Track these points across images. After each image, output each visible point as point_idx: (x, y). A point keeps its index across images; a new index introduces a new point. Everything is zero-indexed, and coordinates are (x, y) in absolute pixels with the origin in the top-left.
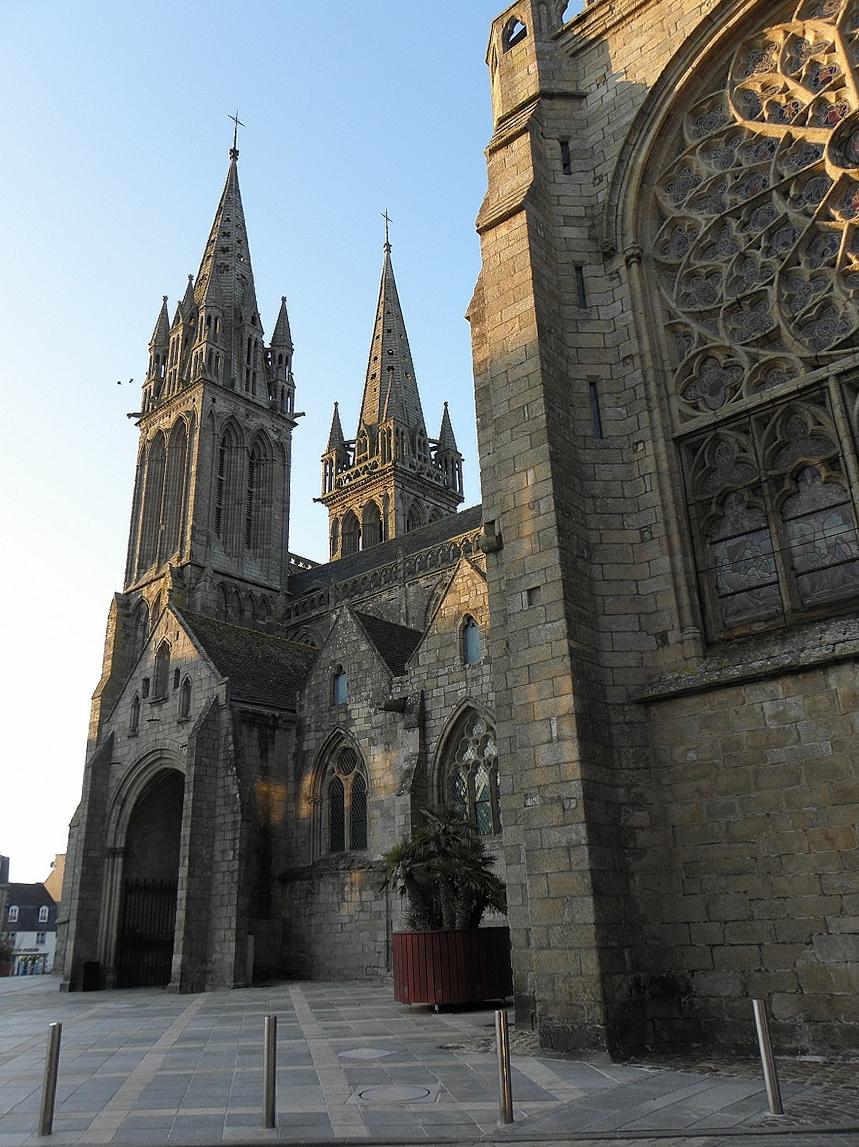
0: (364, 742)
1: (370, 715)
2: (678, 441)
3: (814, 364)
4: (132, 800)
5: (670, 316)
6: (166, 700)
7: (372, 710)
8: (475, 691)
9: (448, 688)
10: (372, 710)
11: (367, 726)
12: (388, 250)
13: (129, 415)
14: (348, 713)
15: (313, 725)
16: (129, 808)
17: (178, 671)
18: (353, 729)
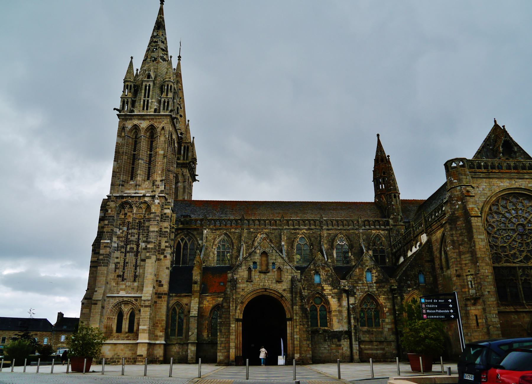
0: (330, 297)
1: (332, 289)
2: (493, 267)
3: (514, 263)
4: (247, 303)
5: (489, 242)
6: (268, 272)
7: (333, 288)
8: (371, 290)
9: (362, 287)
10: (333, 288)
11: (331, 292)
12: (179, 60)
13: (115, 109)
14: (323, 287)
15: (306, 288)
16: (245, 306)
17: (273, 264)
18: (325, 292)
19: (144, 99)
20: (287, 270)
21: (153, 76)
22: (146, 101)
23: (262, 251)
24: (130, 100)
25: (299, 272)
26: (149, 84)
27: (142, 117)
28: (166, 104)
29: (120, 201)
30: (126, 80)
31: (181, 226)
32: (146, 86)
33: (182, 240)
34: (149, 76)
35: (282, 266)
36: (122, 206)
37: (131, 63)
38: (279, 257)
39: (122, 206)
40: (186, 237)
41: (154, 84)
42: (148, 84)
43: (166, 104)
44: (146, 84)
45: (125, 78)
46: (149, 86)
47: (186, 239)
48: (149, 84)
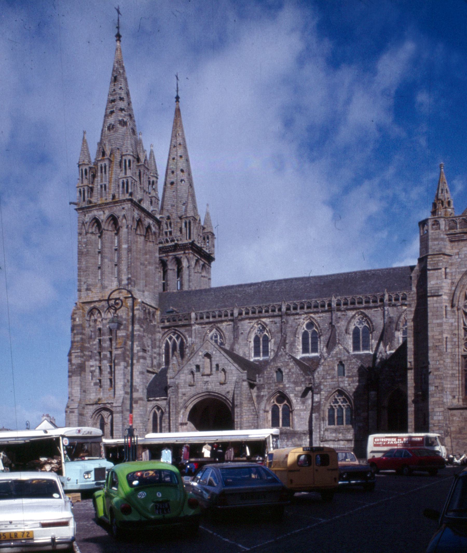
19: (101, 184)
20: (231, 371)
21: (108, 152)
22: (103, 186)
23: (204, 353)
24: (86, 188)
25: (246, 371)
26: (105, 164)
27: (101, 207)
28: (125, 186)
29: (87, 308)
30: (80, 163)
31: (167, 324)
32: (101, 168)
33: (170, 338)
34: (104, 154)
35: (226, 367)
36: (91, 312)
37: (84, 141)
38: (223, 357)
39: (91, 312)
40: (174, 335)
41: (111, 161)
42: (103, 166)
43: (125, 186)
44: (101, 165)
45: (79, 162)
46: (105, 167)
47: (174, 337)
48: (105, 164)
